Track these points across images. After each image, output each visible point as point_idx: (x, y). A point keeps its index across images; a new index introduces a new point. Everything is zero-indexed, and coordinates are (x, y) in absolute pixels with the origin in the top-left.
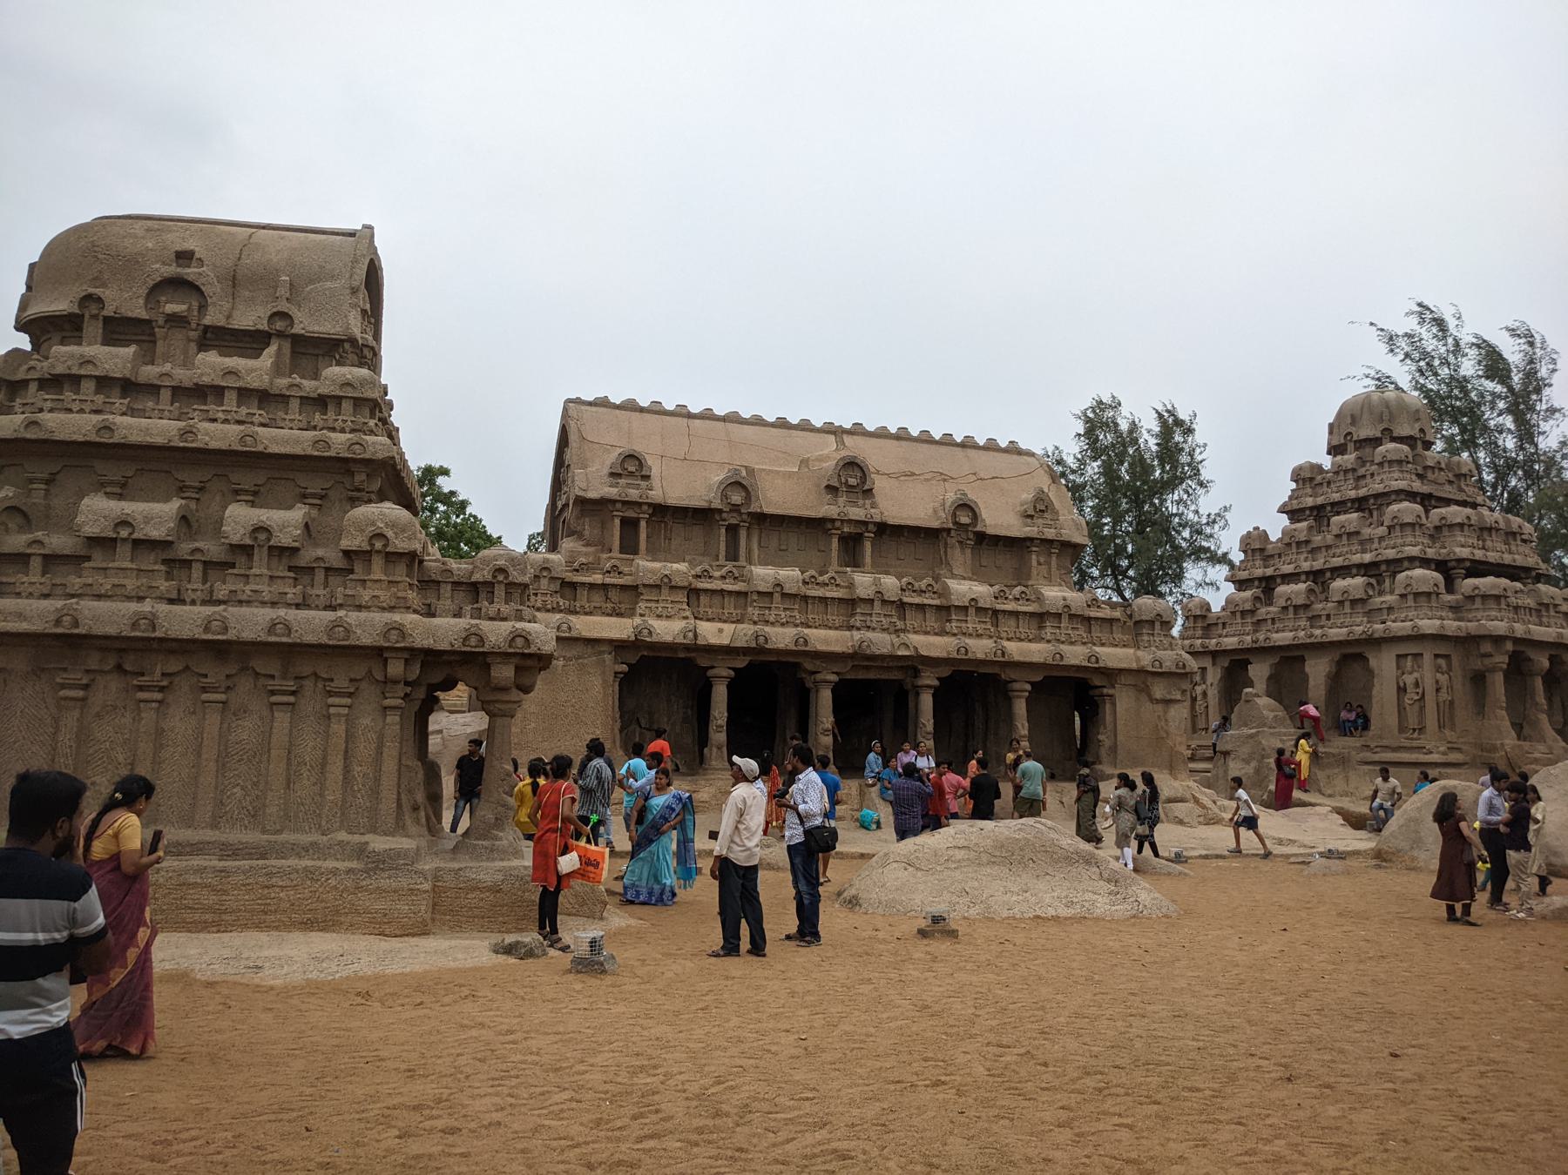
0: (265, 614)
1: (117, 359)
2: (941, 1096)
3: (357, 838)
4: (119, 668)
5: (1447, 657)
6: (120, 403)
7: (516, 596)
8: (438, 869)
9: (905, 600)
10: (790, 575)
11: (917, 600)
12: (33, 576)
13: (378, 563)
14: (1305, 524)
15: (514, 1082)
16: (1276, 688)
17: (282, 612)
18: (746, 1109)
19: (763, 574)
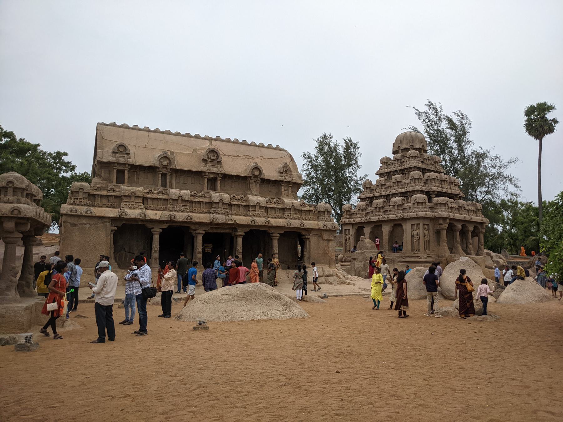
5: (428, 225)
9: (232, 203)
10: (186, 193)
11: (237, 203)
14: (384, 178)
16: (373, 237)
19: (174, 192)
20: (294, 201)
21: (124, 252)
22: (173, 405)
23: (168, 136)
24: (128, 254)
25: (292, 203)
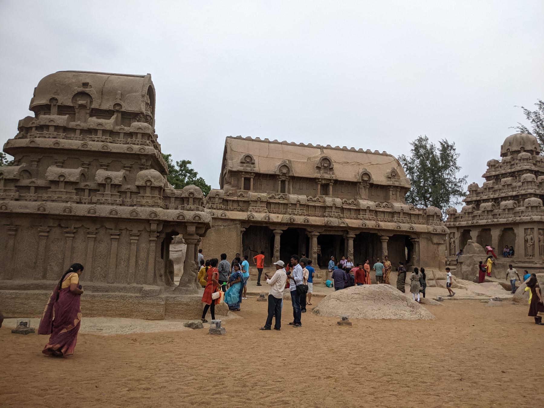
0: (109, 208)
1: (61, 120)
2: (328, 382)
3: (140, 286)
4: (60, 226)
6: (62, 134)
7: (197, 202)
8: (167, 297)
9: (344, 207)
10: (303, 198)
11: (348, 207)
12: (32, 194)
13: (148, 190)
15: (176, 372)
17: (115, 207)
18: (255, 384)
19: (293, 197)
22: (373, 388)
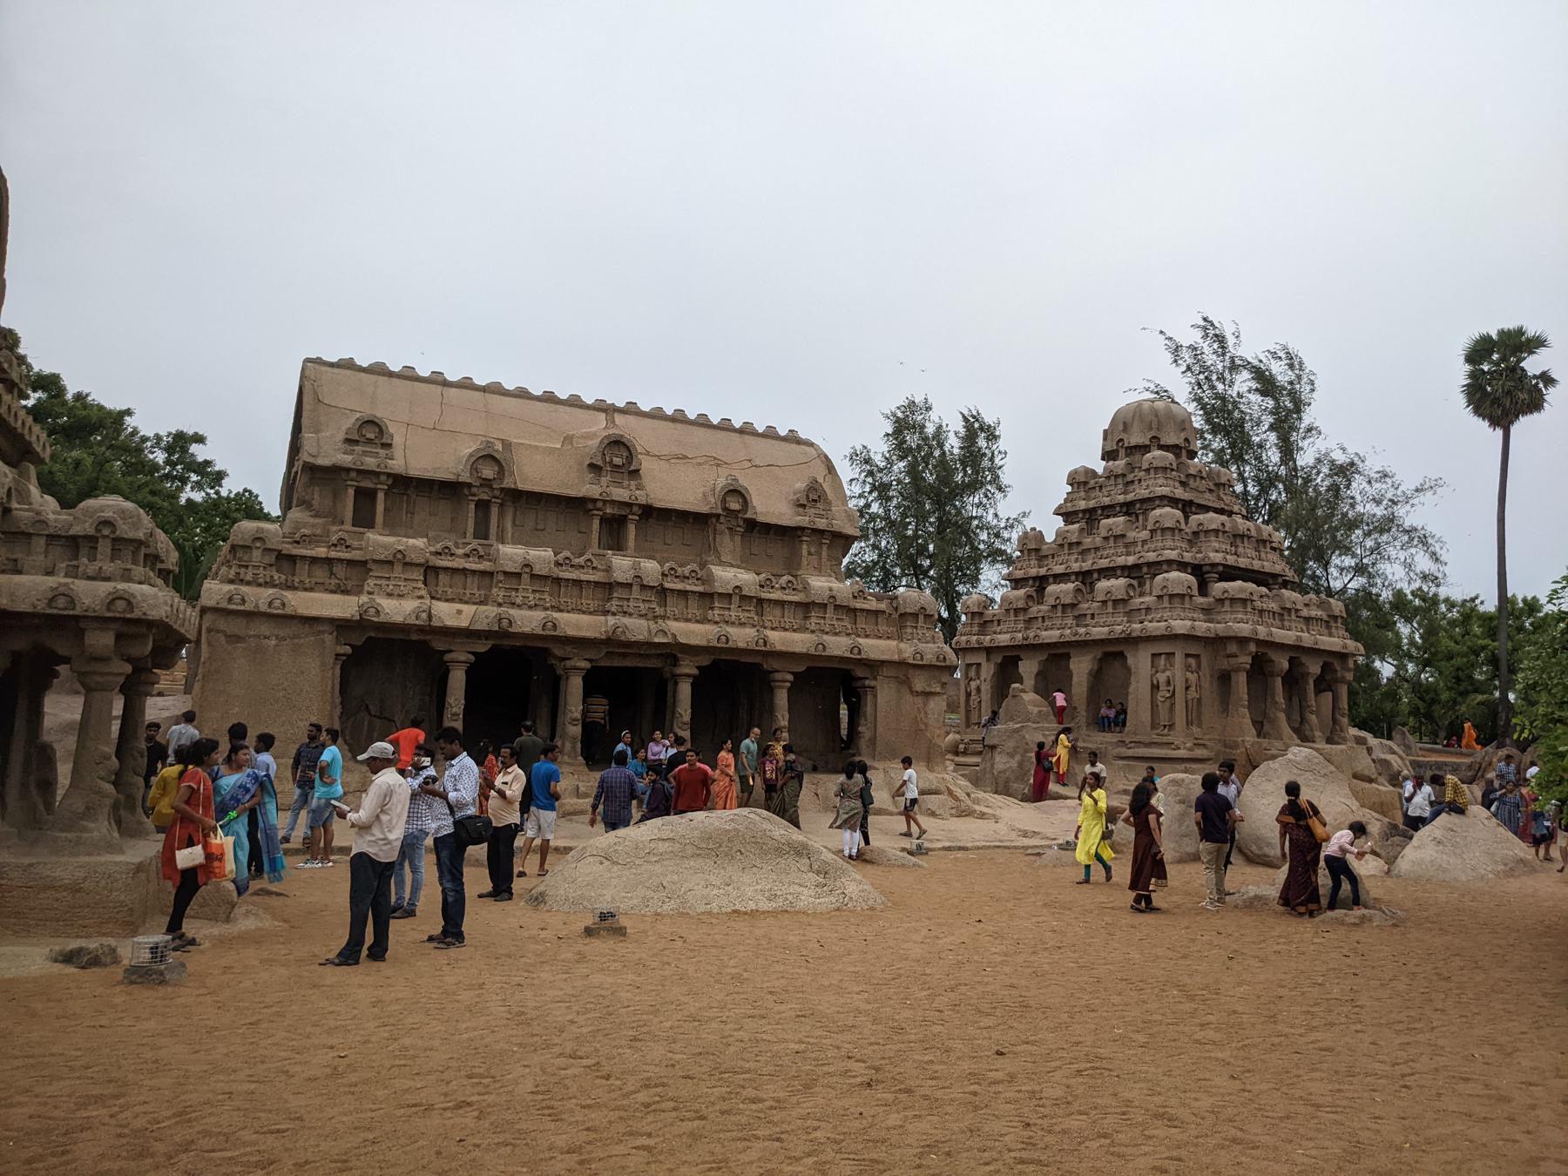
5: (1197, 656)
9: (667, 585)
10: (542, 556)
11: (679, 586)
14: (1076, 526)
16: (1045, 686)
18: (186, 1147)
19: (511, 553)
20: (836, 585)
21: (367, 718)
22: (588, 1129)
23: (495, 399)
24: (378, 723)
25: (831, 589)
